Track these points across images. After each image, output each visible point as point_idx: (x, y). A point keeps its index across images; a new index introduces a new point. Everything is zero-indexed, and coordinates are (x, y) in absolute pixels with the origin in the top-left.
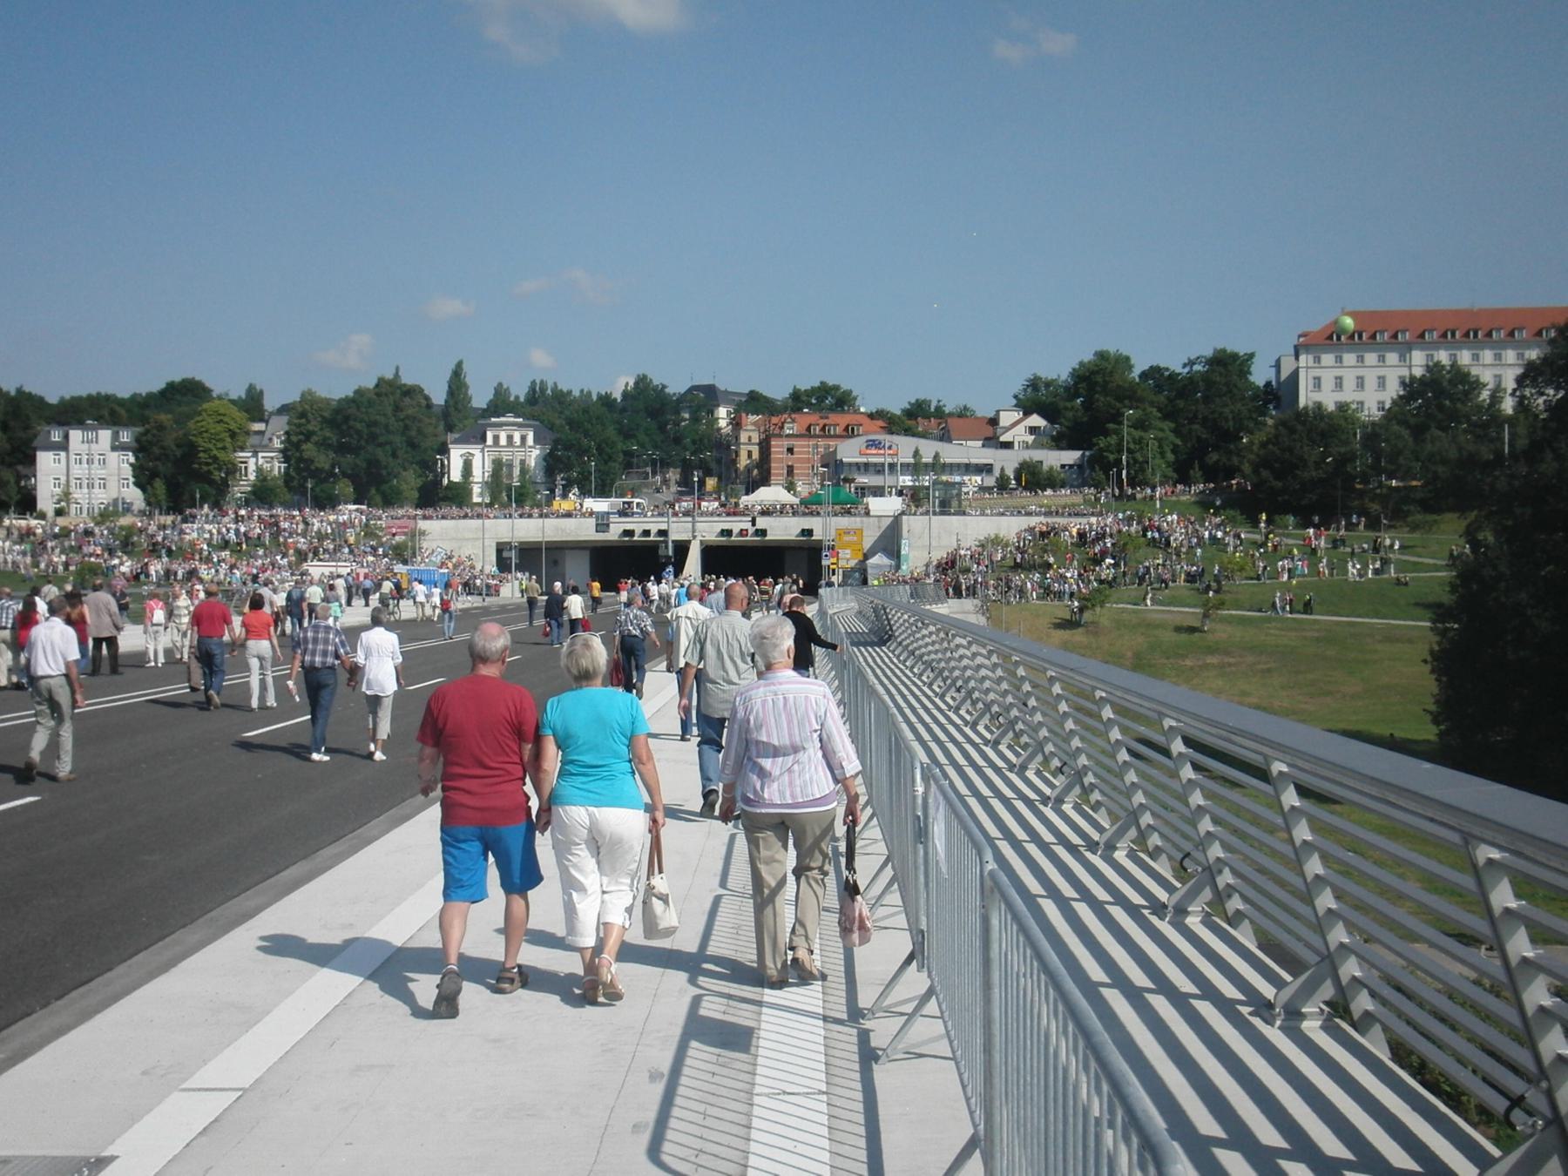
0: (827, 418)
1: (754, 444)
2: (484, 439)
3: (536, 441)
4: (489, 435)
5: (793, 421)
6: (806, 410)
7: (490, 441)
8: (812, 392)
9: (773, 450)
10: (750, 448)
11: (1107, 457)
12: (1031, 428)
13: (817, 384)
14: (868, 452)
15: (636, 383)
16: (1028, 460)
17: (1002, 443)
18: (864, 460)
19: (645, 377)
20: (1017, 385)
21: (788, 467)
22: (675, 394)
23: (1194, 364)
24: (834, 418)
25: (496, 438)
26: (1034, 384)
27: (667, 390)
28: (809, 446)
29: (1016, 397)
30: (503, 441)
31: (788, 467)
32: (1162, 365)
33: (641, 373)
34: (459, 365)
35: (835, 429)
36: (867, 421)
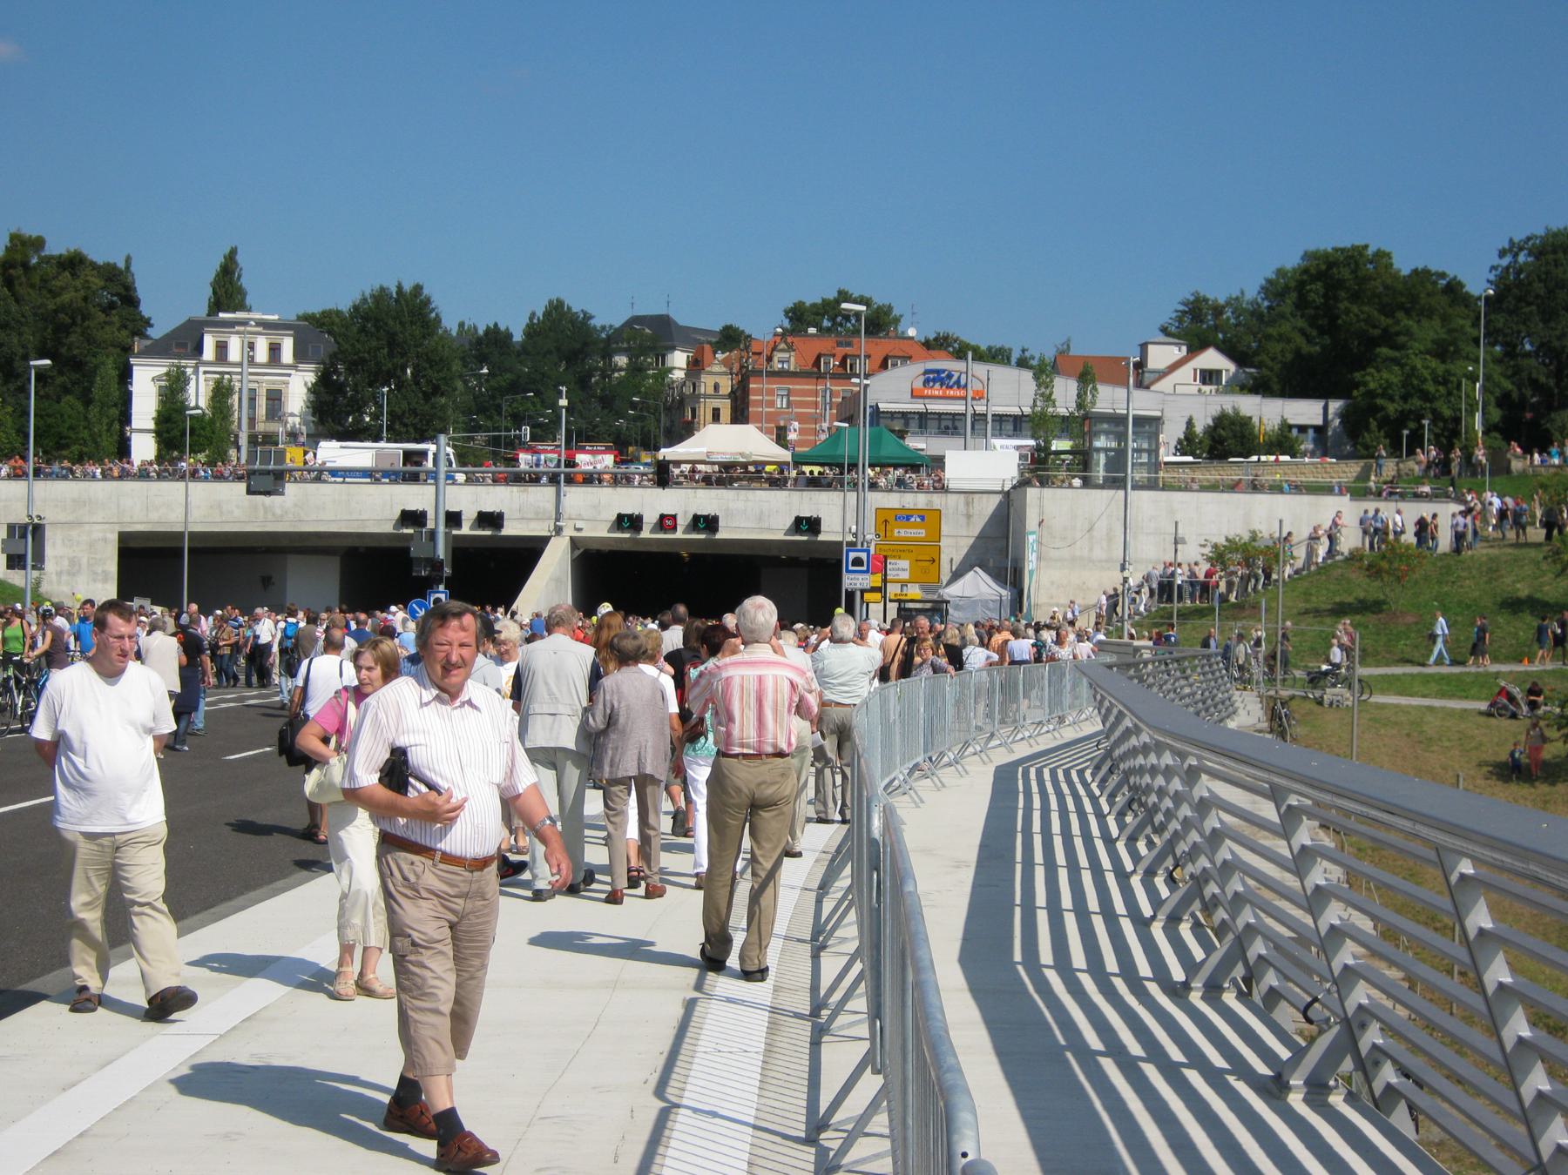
1: (723, 397)
2: (199, 349)
3: (300, 355)
4: (209, 343)
7: (209, 352)
9: (752, 398)
10: (716, 403)
11: (1382, 408)
12: (1202, 371)
14: (928, 392)
15: (547, 314)
16: (1230, 411)
18: (918, 407)
19: (560, 303)
20: (1167, 309)
22: (603, 328)
25: (222, 348)
27: (592, 322)
30: (234, 354)
32: (1434, 268)
33: (554, 297)
34: (231, 257)
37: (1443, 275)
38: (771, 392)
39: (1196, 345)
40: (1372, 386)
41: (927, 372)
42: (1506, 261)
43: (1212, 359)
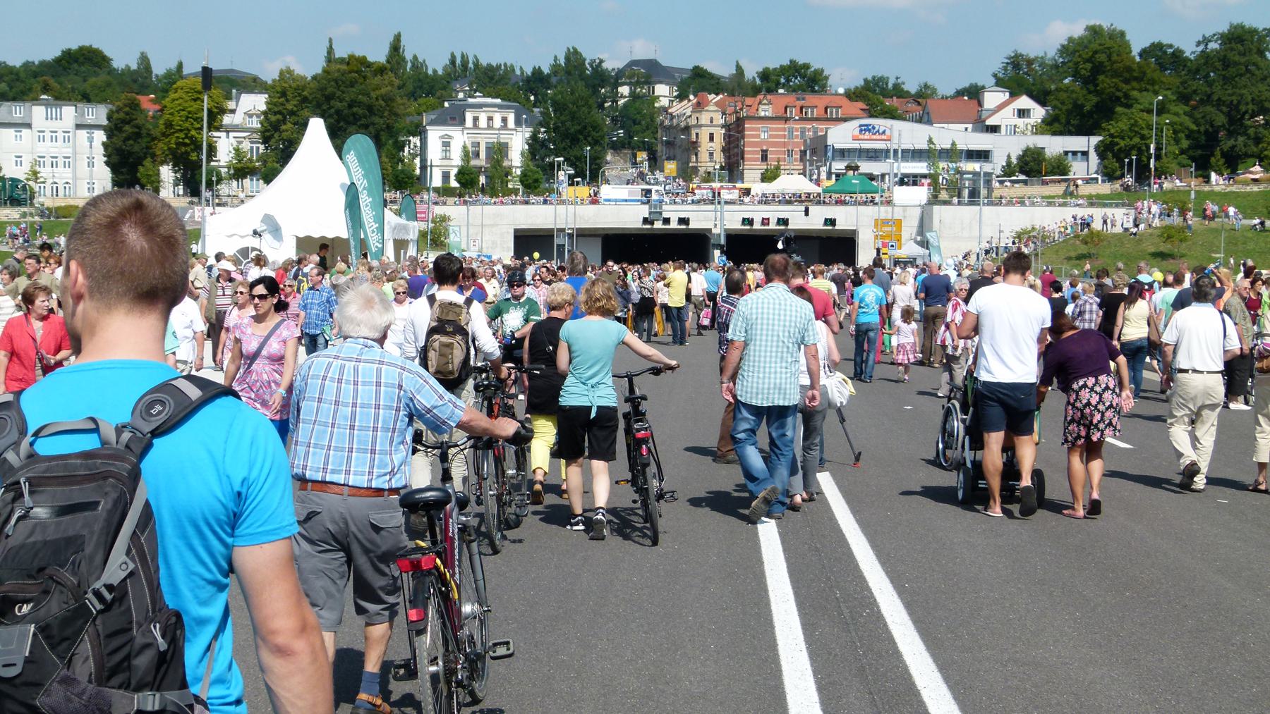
0: (803, 99)
2: (462, 122)
3: (518, 122)
4: (469, 116)
5: (770, 103)
6: (781, 91)
8: (783, 70)
9: (746, 133)
10: (712, 130)
12: (1019, 111)
13: (786, 62)
16: (1032, 146)
17: (988, 126)
20: (996, 62)
21: (763, 151)
23: (1210, 41)
24: (811, 99)
26: (1016, 62)
28: (784, 130)
29: (995, 76)
30: (483, 122)
31: (763, 151)
32: (1165, 42)
35: (812, 112)
36: (845, 102)
37: (1171, 46)
38: (757, 130)
39: (1014, 95)
40: (1112, 131)
41: (860, 126)
42: (1201, 48)
43: (1024, 102)
